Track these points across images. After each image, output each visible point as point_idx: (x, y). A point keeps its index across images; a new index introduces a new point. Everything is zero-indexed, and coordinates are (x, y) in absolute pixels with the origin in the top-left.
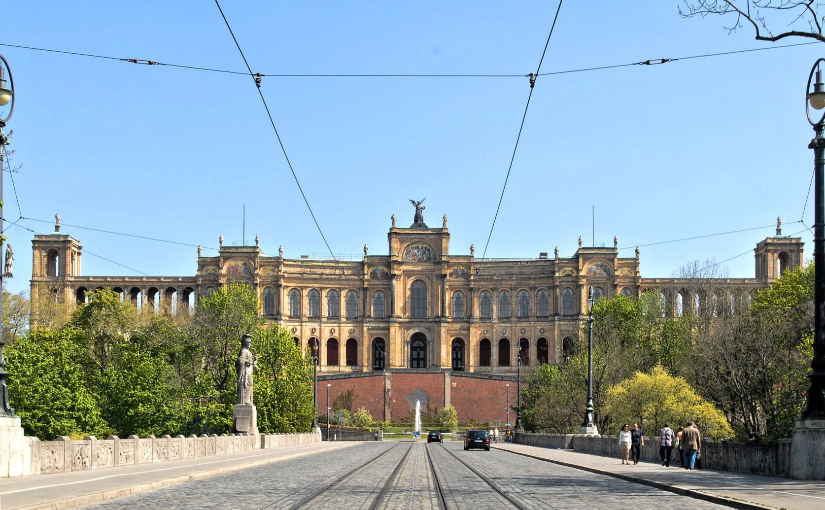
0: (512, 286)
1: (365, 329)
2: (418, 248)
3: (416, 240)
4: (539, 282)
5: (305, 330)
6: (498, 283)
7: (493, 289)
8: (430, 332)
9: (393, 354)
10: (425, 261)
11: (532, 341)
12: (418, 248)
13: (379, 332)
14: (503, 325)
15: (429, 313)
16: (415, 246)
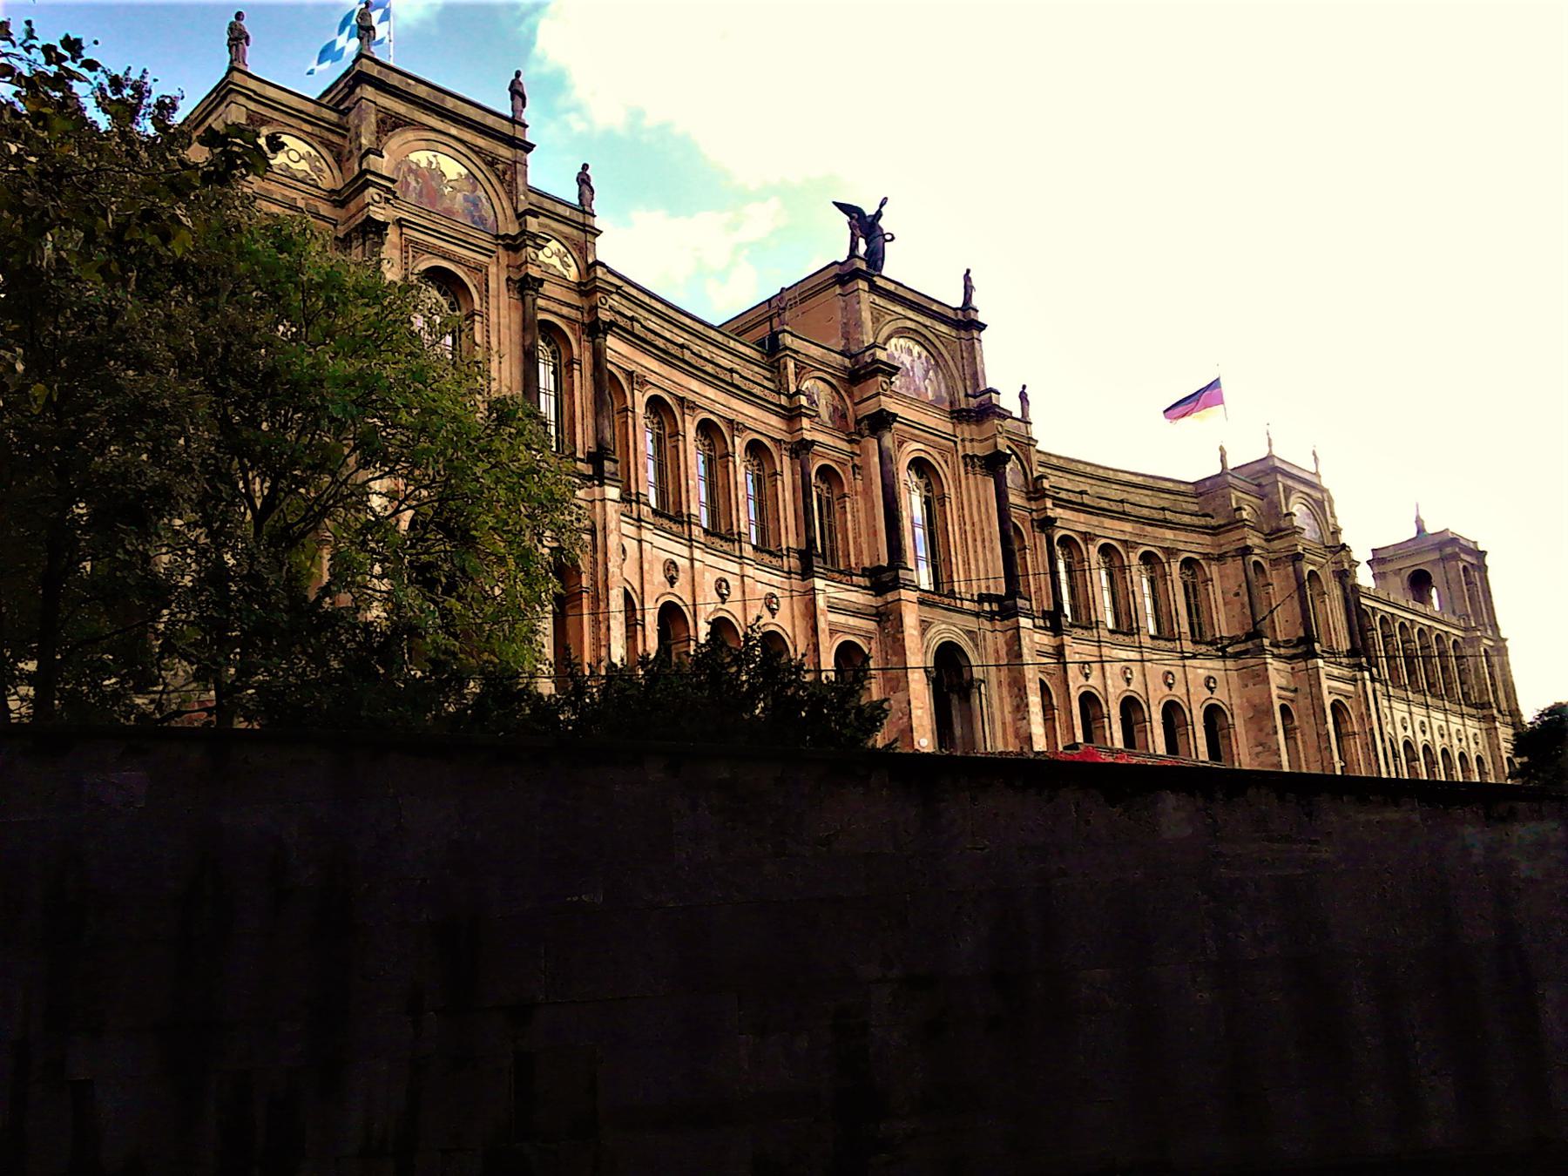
0: (1127, 538)
1: (821, 602)
2: (910, 352)
3: (909, 324)
4: (1182, 536)
5: (651, 563)
6: (1094, 520)
7: (1088, 537)
8: (976, 645)
9: (919, 712)
10: (930, 404)
11: (1194, 712)
12: (910, 352)
13: (852, 621)
14: (1123, 655)
15: (960, 587)
16: (902, 341)
